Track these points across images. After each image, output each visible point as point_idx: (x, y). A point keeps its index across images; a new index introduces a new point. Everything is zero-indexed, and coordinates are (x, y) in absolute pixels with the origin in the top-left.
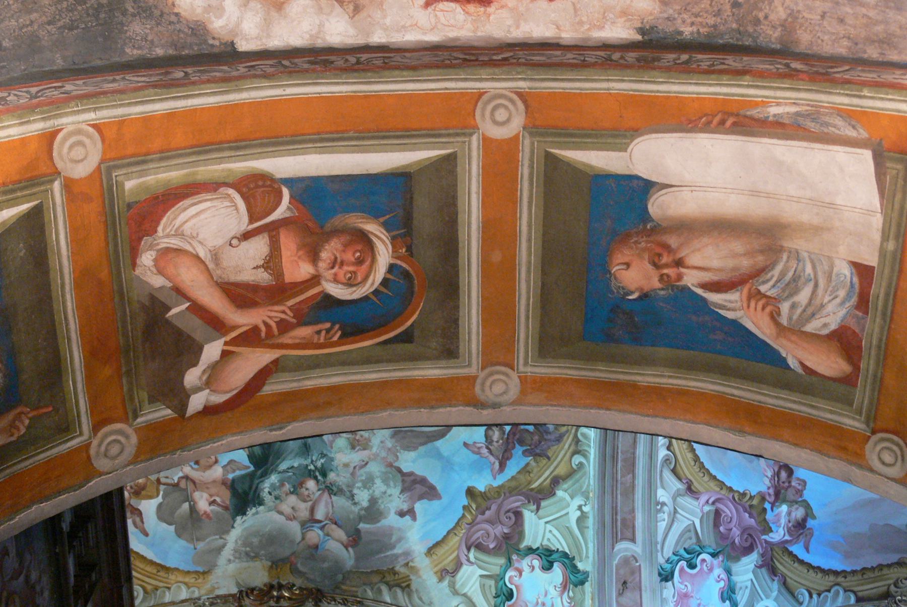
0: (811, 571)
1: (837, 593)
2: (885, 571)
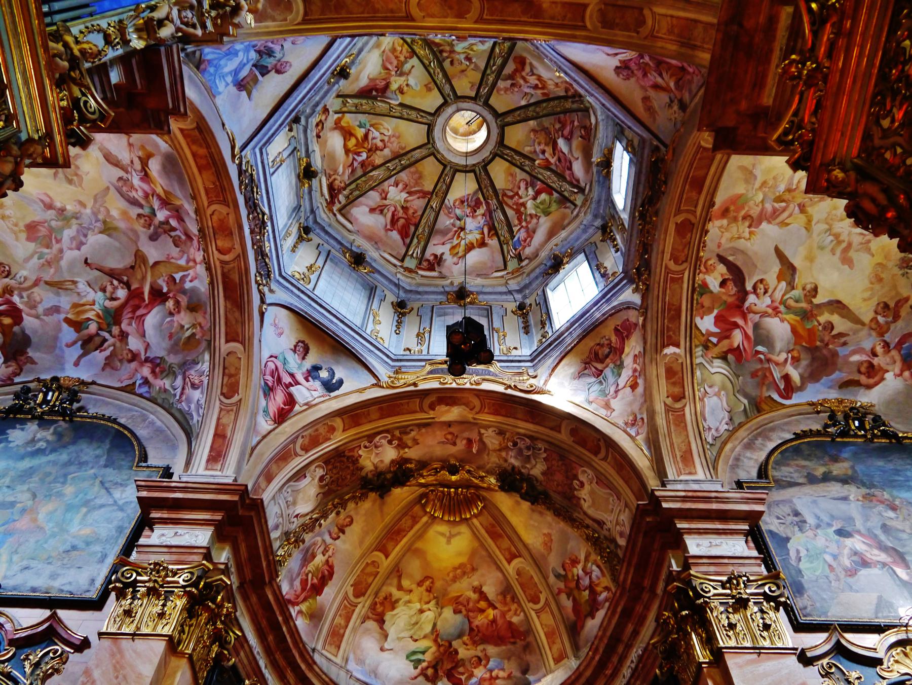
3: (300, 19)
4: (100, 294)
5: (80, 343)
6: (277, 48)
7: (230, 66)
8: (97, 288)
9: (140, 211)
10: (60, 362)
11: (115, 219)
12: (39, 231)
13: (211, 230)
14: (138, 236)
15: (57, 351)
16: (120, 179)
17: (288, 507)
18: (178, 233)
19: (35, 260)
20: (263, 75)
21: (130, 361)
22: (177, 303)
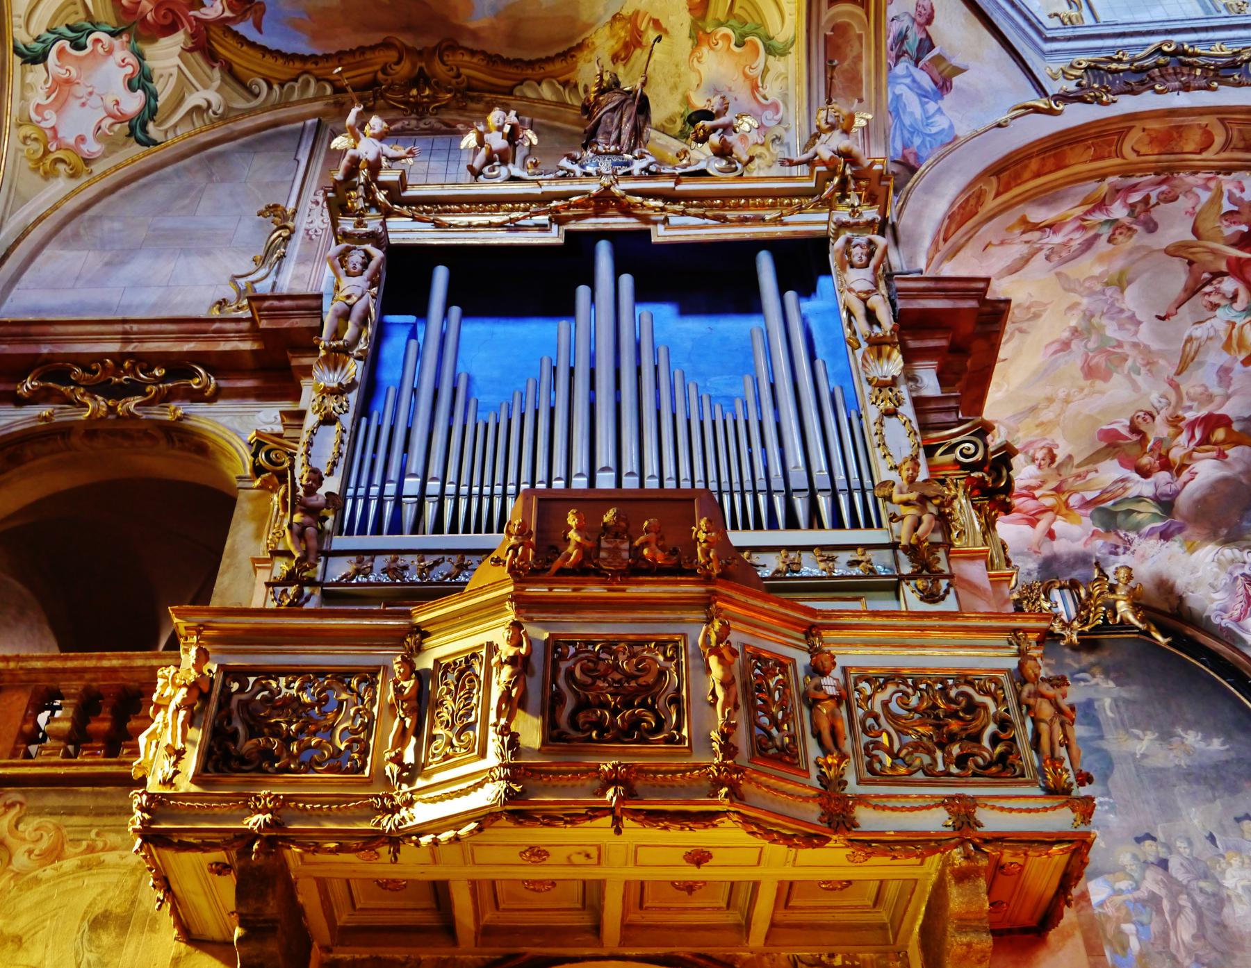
0: (267, 56)
1: (307, 83)
2: (368, 55)
3: (859, 11)
4: (1219, 312)
7: (912, 103)
8: (1210, 314)
9: (1104, 238)
11: (1107, 271)
12: (1097, 365)
13: (1164, 157)
14: (1143, 247)
16: (1048, 258)
18: (1154, 195)
19: (1140, 380)
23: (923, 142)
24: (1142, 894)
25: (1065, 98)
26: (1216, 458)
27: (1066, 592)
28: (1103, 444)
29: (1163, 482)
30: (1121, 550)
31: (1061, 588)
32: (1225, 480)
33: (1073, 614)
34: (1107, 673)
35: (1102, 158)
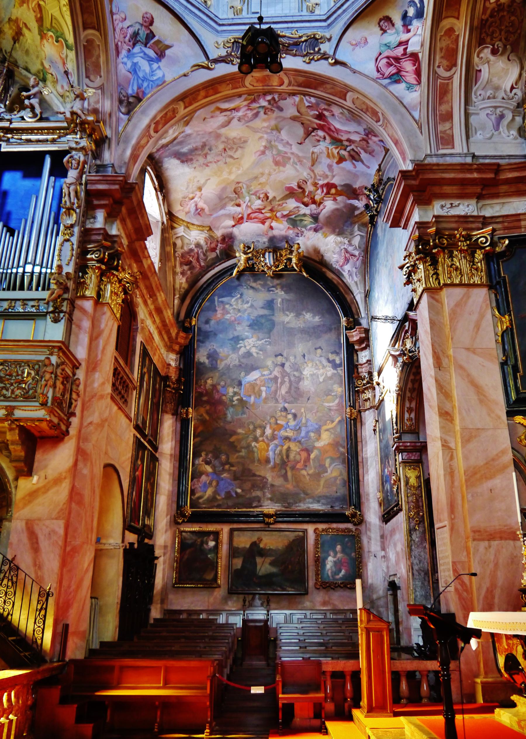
3: (97, 33)
4: (321, 143)
5: (354, 161)
6: (130, 31)
7: (144, 66)
8: (318, 143)
10: (366, 175)
12: (279, 160)
13: (265, 87)
14: (280, 117)
15: (357, 173)
16: (239, 120)
17: (494, 98)
20: (154, 36)
21: (368, 143)
22: (325, 109)
23: (148, 85)
24: (272, 376)
25: (216, 61)
26: (333, 200)
27: (271, 254)
28: (288, 192)
29: (313, 209)
30: (300, 235)
31: (269, 252)
32: (337, 210)
33: (272, 264)
34: (282, 288)
35: (237, 88)
